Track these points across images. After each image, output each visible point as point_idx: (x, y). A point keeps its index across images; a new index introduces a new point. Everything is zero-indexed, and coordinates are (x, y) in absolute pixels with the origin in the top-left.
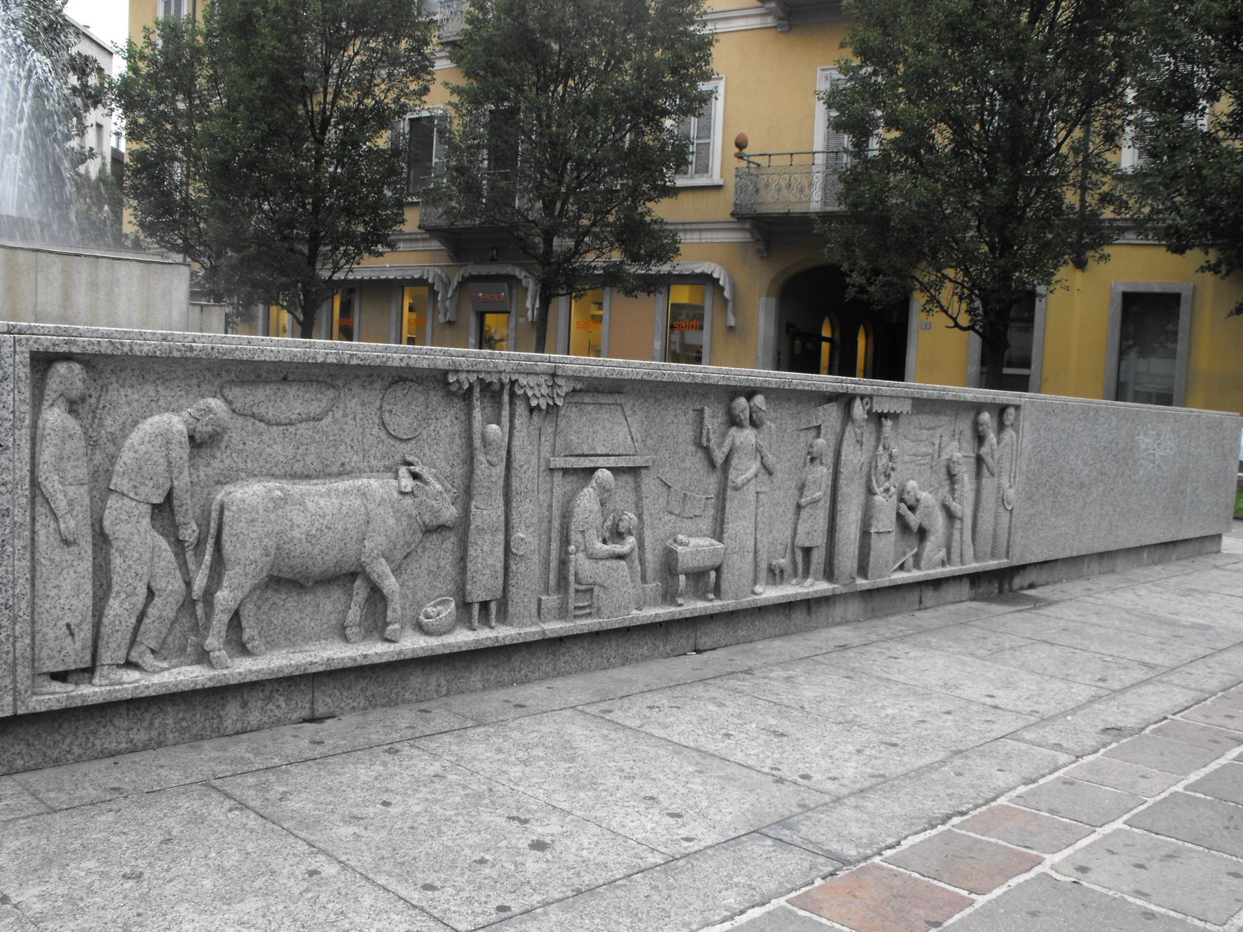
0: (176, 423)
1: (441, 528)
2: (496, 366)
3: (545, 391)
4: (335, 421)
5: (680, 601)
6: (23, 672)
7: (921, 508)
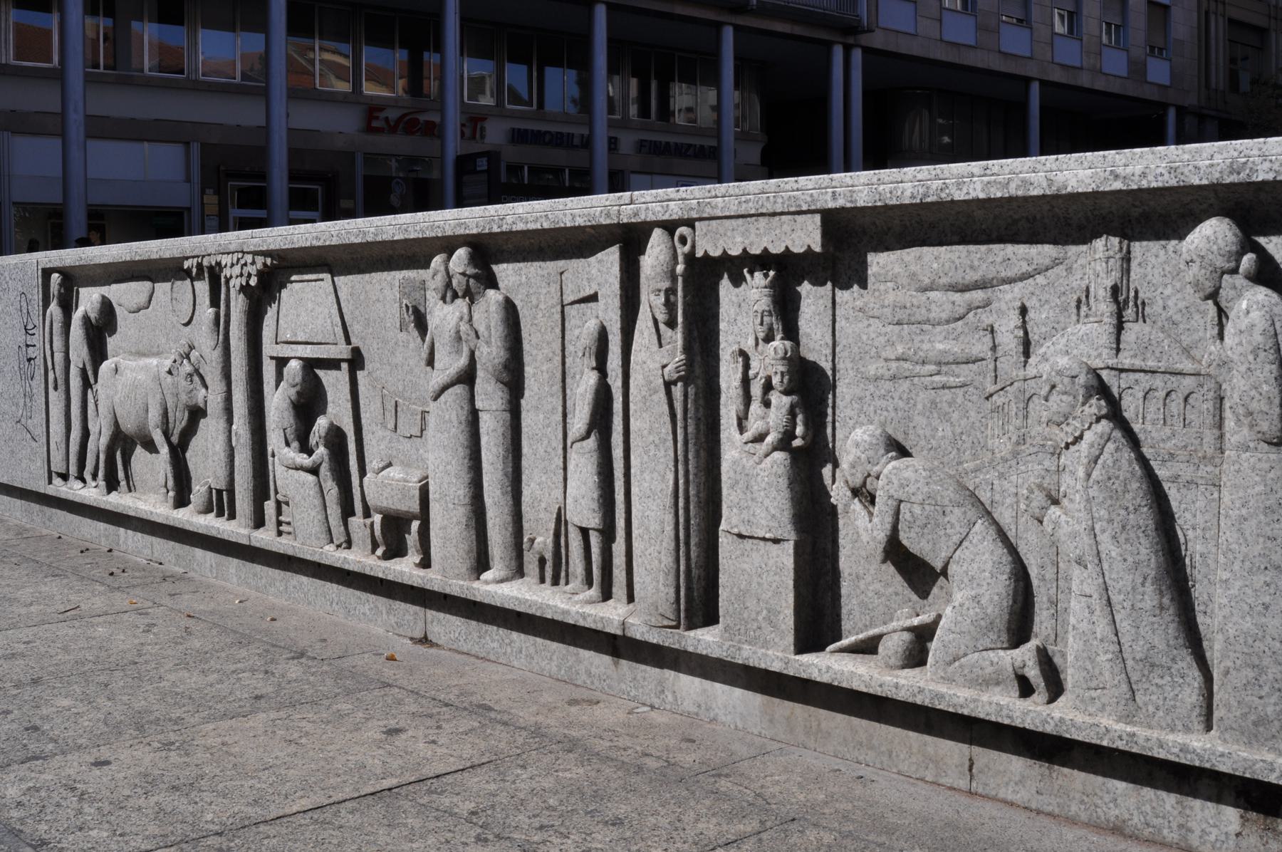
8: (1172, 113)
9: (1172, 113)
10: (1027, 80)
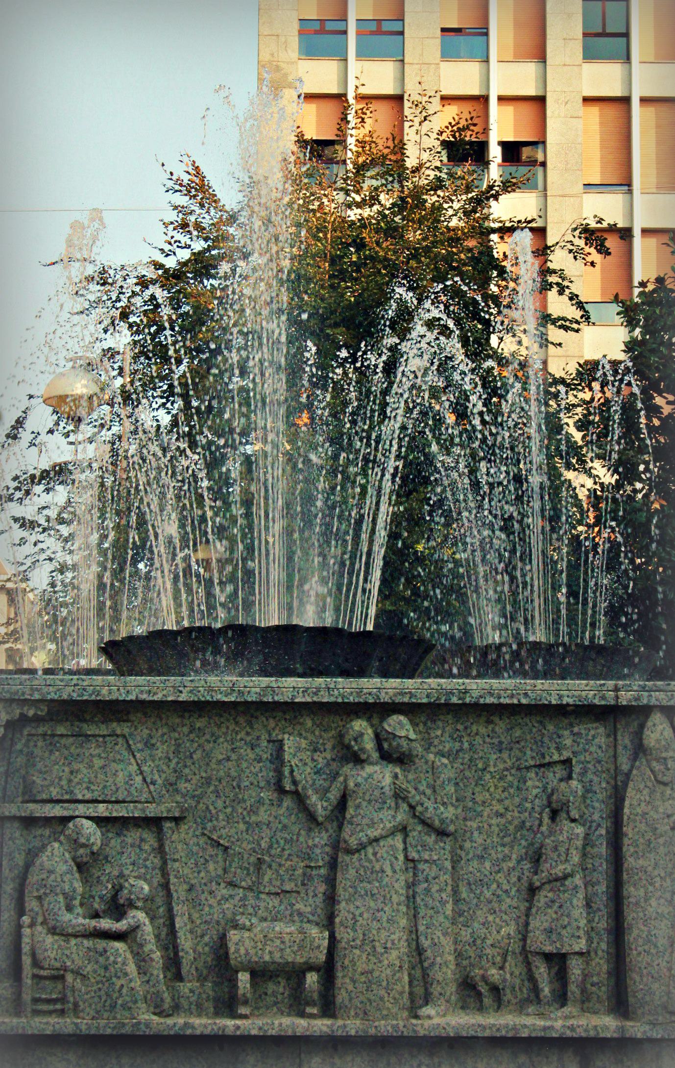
5: (243, 1010)
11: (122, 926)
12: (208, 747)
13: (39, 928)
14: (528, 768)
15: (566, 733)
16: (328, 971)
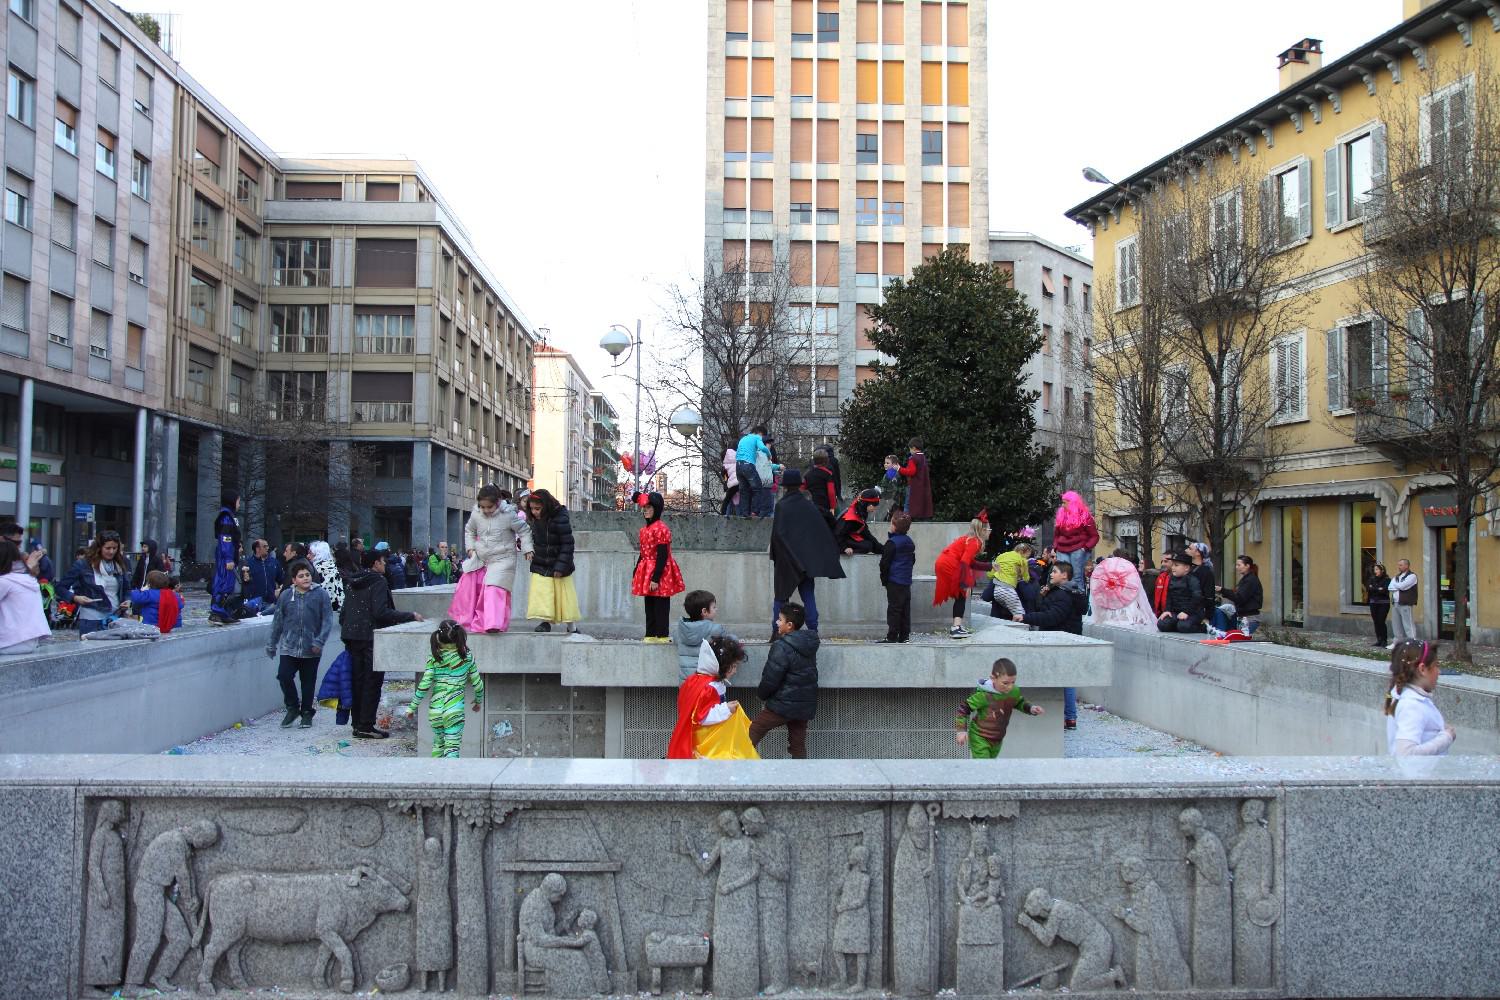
0: (174, 835)
1: (392, 912)
2: (430, 795)
3: (480, 812)
4: (305, 833)
6: (74, 983)
7: (1052, 920)
8: (143, 416)
9: (143, 416)
10: (22, 379)
11: (579, 941)
12: (633, 825)
13: (528, 942)
14: (835, 837)
15: (860, 816)
16: (708, 967)
